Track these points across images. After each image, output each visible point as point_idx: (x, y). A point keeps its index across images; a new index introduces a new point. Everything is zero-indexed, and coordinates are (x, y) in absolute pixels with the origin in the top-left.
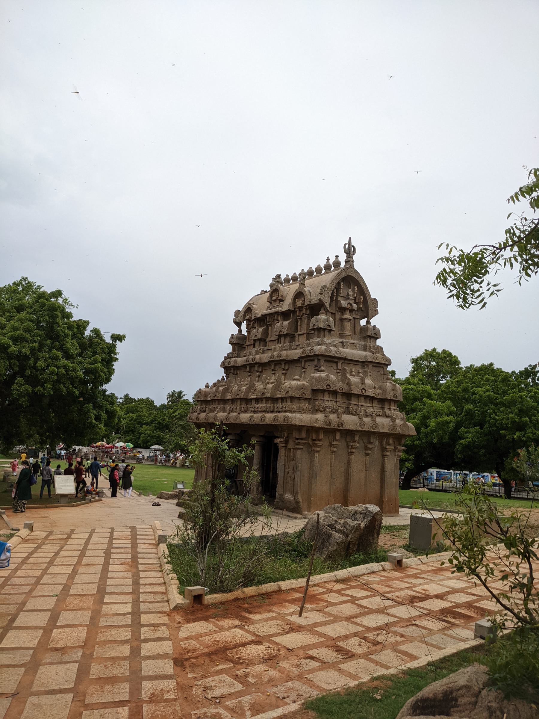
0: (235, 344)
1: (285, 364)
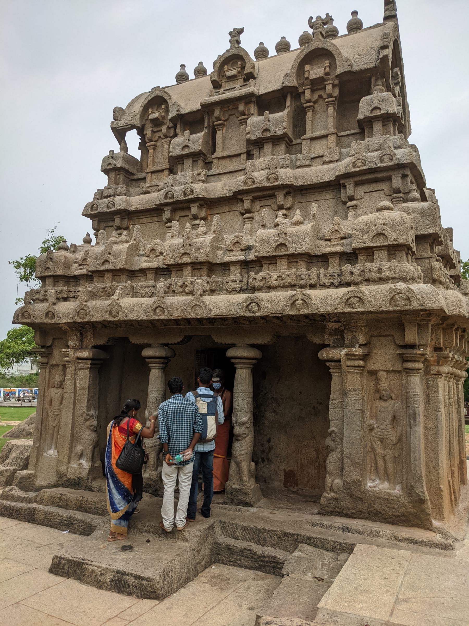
0: (120, 169)
1: (285, 196)
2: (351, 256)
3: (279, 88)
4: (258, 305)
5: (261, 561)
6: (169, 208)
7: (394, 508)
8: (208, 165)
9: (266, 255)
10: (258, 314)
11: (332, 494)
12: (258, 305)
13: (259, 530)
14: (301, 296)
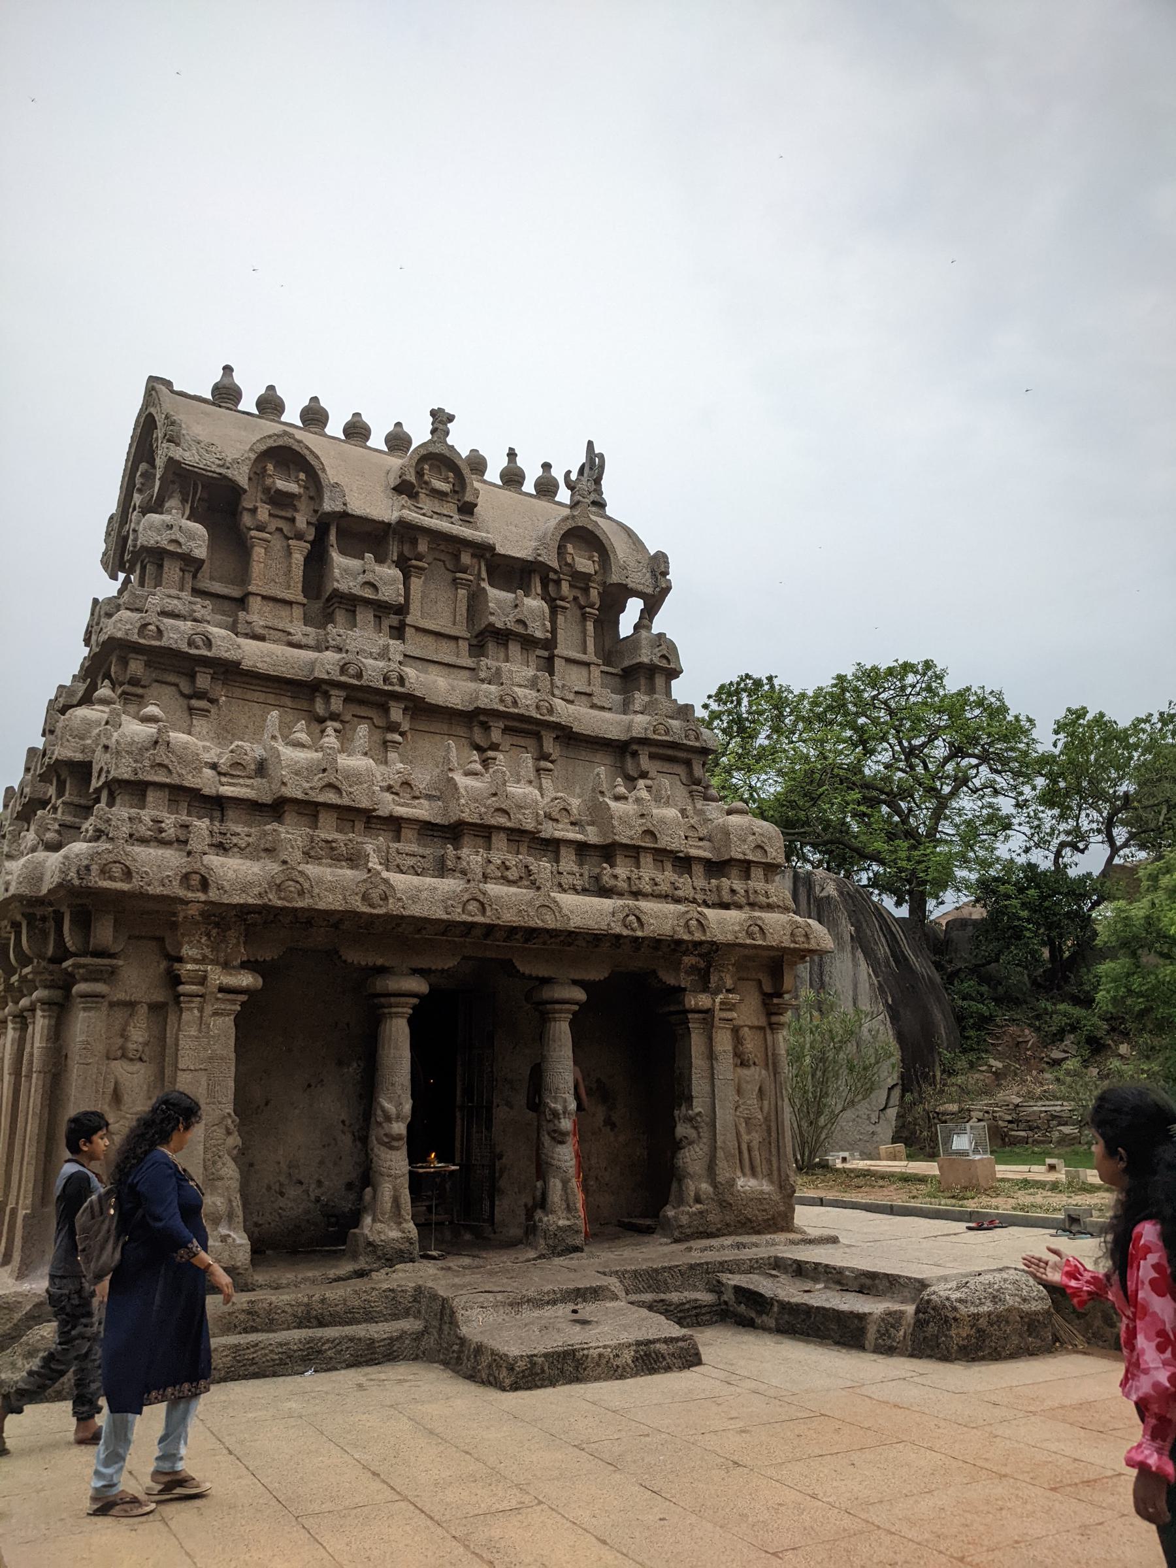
2: (716, 868)
3: (530, 558)
4: (638, 919)
5: (680, 1311)
6: (343, 694)
7: (765, 1210)
8: (398, 632)
9: (628, 842)
10: (639, 934)
11: (698, 1206)
12: (638, 919)
13: (656, 1270)
14: (696, 915)
